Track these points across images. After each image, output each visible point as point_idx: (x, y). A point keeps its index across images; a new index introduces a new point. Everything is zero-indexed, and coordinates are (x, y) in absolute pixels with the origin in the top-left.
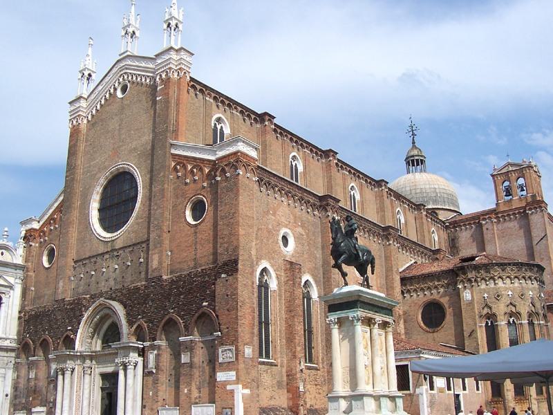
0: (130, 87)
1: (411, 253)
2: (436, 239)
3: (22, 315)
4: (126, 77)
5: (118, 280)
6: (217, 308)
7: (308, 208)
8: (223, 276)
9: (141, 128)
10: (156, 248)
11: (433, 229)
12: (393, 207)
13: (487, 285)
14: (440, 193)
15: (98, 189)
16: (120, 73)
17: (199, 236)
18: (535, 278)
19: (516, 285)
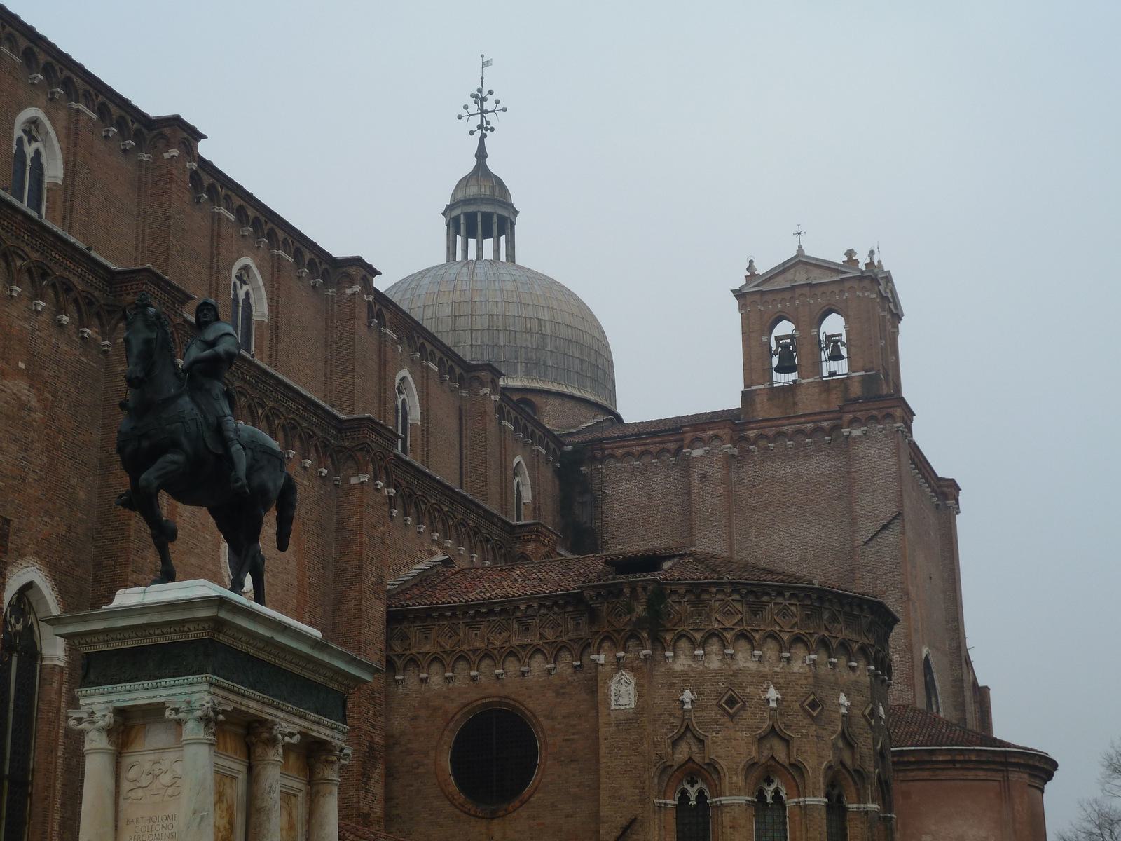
1: (433, 529)
2: (527, 495)
7: (61, 310)
11: (518, 459)
12: (383, 364)
13: (694, 658)
14: (555, 337)
18: (863, 650)
19: (797, 667)
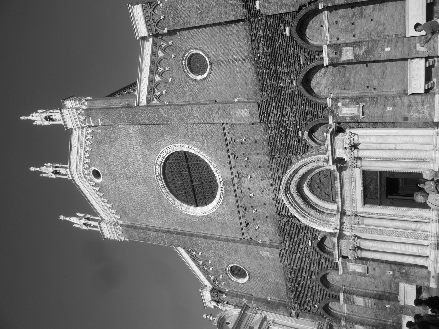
0: (95, 166)
3: (293, 312)
4: (86, 172)
5: (262, 174)
6: (292, 9)
8: (258, 7)
9: (126, 148)
10: (229, 114)
15: (177, 204)
16: (84, 178)
17: (221, 58)
